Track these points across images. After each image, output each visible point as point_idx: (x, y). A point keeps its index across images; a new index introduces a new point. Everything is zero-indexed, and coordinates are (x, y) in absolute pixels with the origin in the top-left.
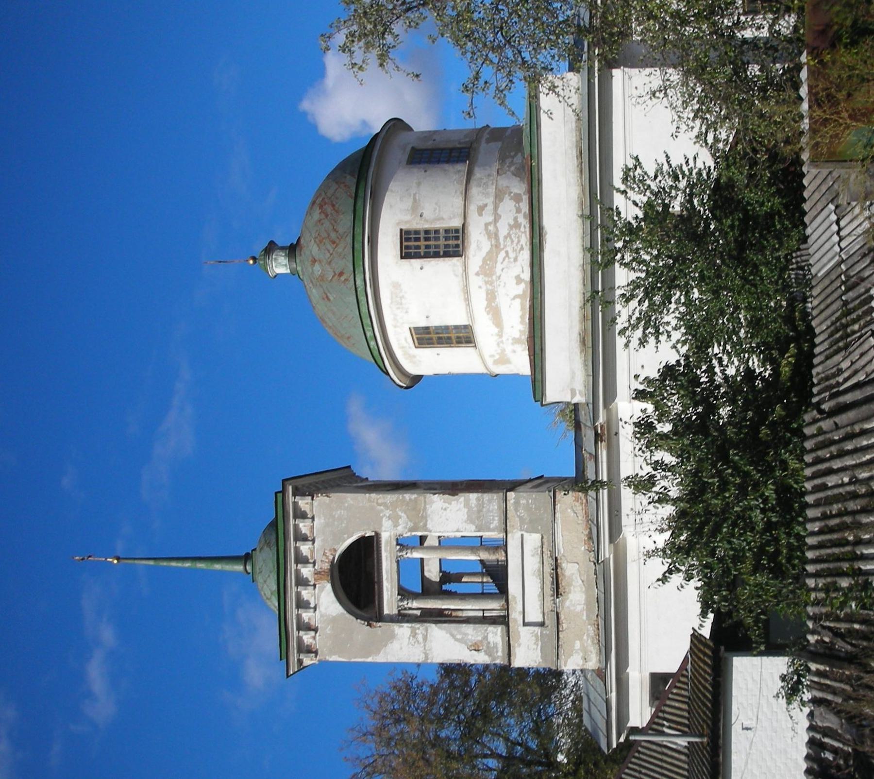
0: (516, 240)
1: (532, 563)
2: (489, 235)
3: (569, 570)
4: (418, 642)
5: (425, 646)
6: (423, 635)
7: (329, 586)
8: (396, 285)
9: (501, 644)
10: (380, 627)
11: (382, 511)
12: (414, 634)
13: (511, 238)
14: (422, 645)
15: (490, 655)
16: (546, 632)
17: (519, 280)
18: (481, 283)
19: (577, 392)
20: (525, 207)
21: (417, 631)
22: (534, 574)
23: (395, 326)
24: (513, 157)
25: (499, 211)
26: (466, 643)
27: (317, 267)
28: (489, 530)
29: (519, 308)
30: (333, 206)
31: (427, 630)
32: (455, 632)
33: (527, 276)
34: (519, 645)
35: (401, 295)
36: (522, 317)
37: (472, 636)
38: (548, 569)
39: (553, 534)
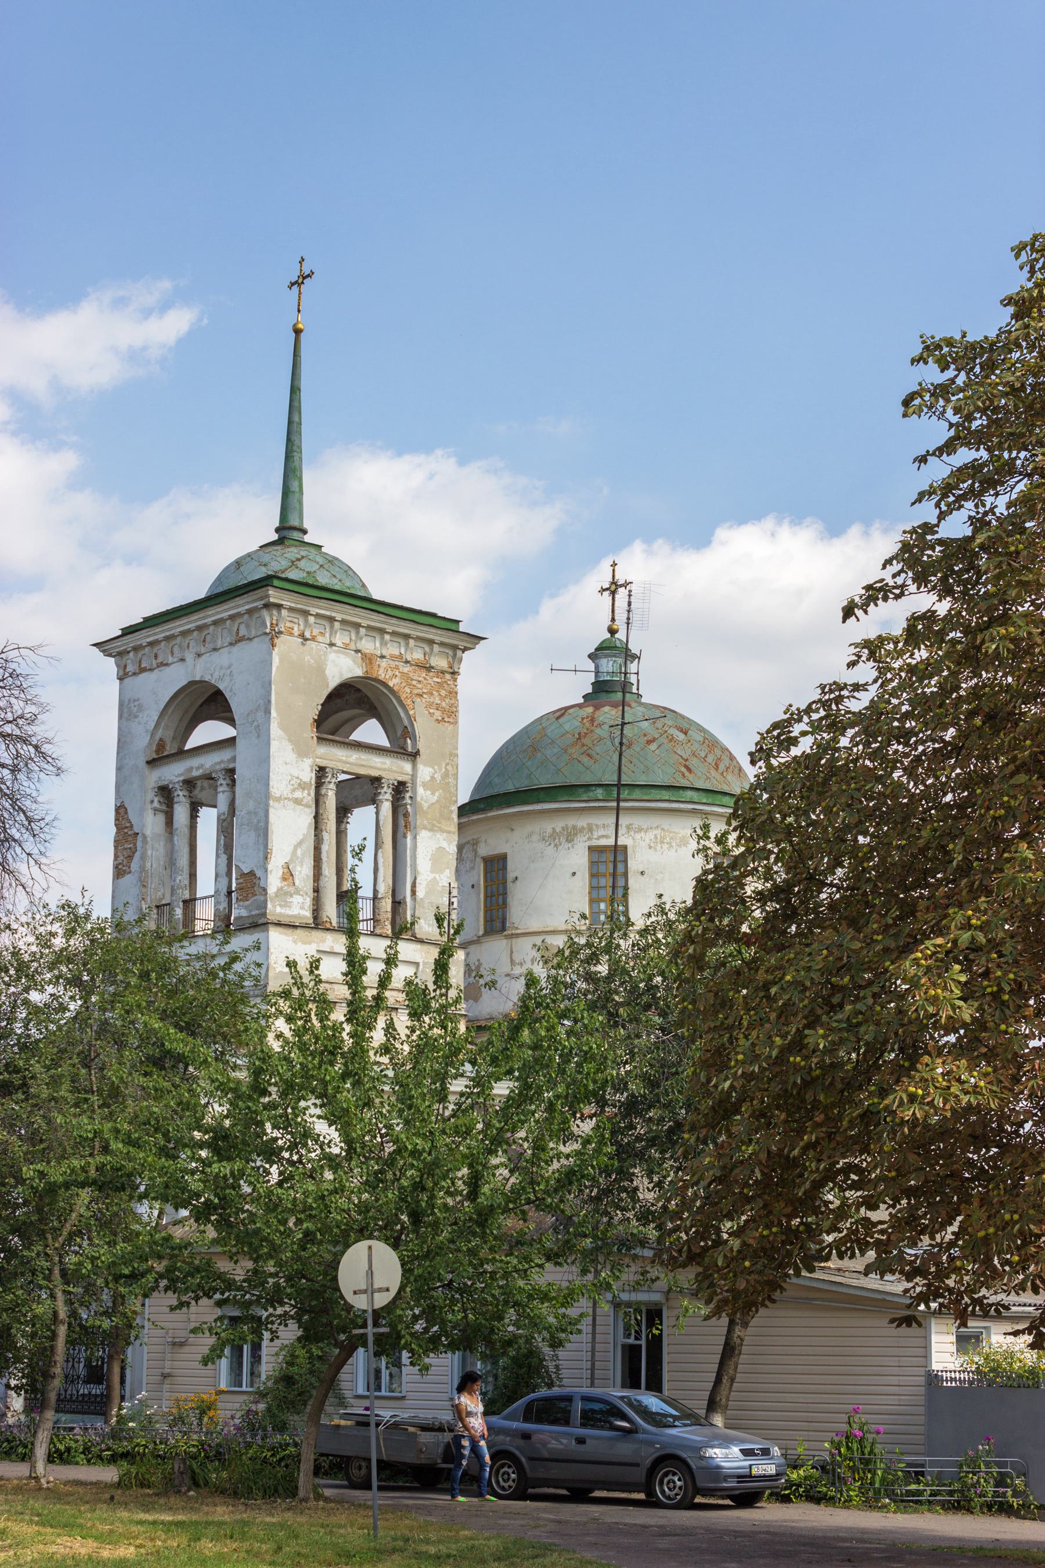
4: (293, 790)
5: (289, 799)
6: (302, 800)
9: (290, 913)
11: (440, 770)
12: (302, 786)
14: (290, 796)
15: (277, 895)
26: (291, 860)
31: (307, 806)
32: (304, 846)
34: (295, 942)
35: (674, 844)
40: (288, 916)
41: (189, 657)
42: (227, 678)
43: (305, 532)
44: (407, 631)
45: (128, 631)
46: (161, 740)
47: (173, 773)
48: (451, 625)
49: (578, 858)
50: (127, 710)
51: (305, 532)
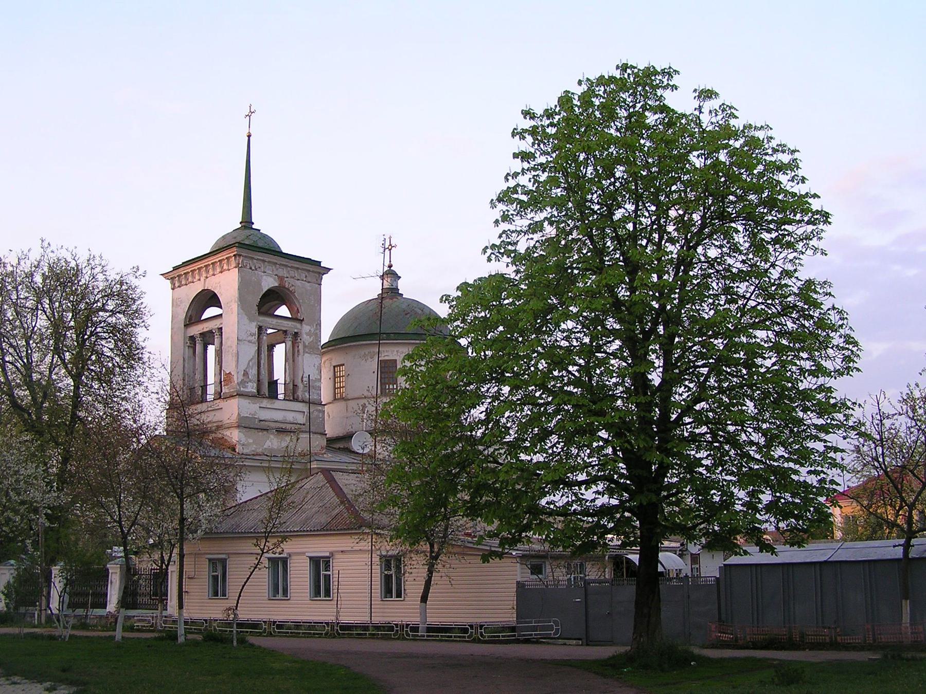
1: (290, 417)
7: (276, 284)
9: (247, 390)
12: (252, 335)
26: (246, 368)
32: (253, 361)
34: (249, 403)
38: (288, 427)
41: (202, 279)
42: (218, 287)
43: (253, 223)
44: (298, 266)
45: (175, 268)
46: (190, 316)
47: (196, 330)
48: (318, 263)
49: (374, 365)
50: (175, 303)
51: (253, 223)
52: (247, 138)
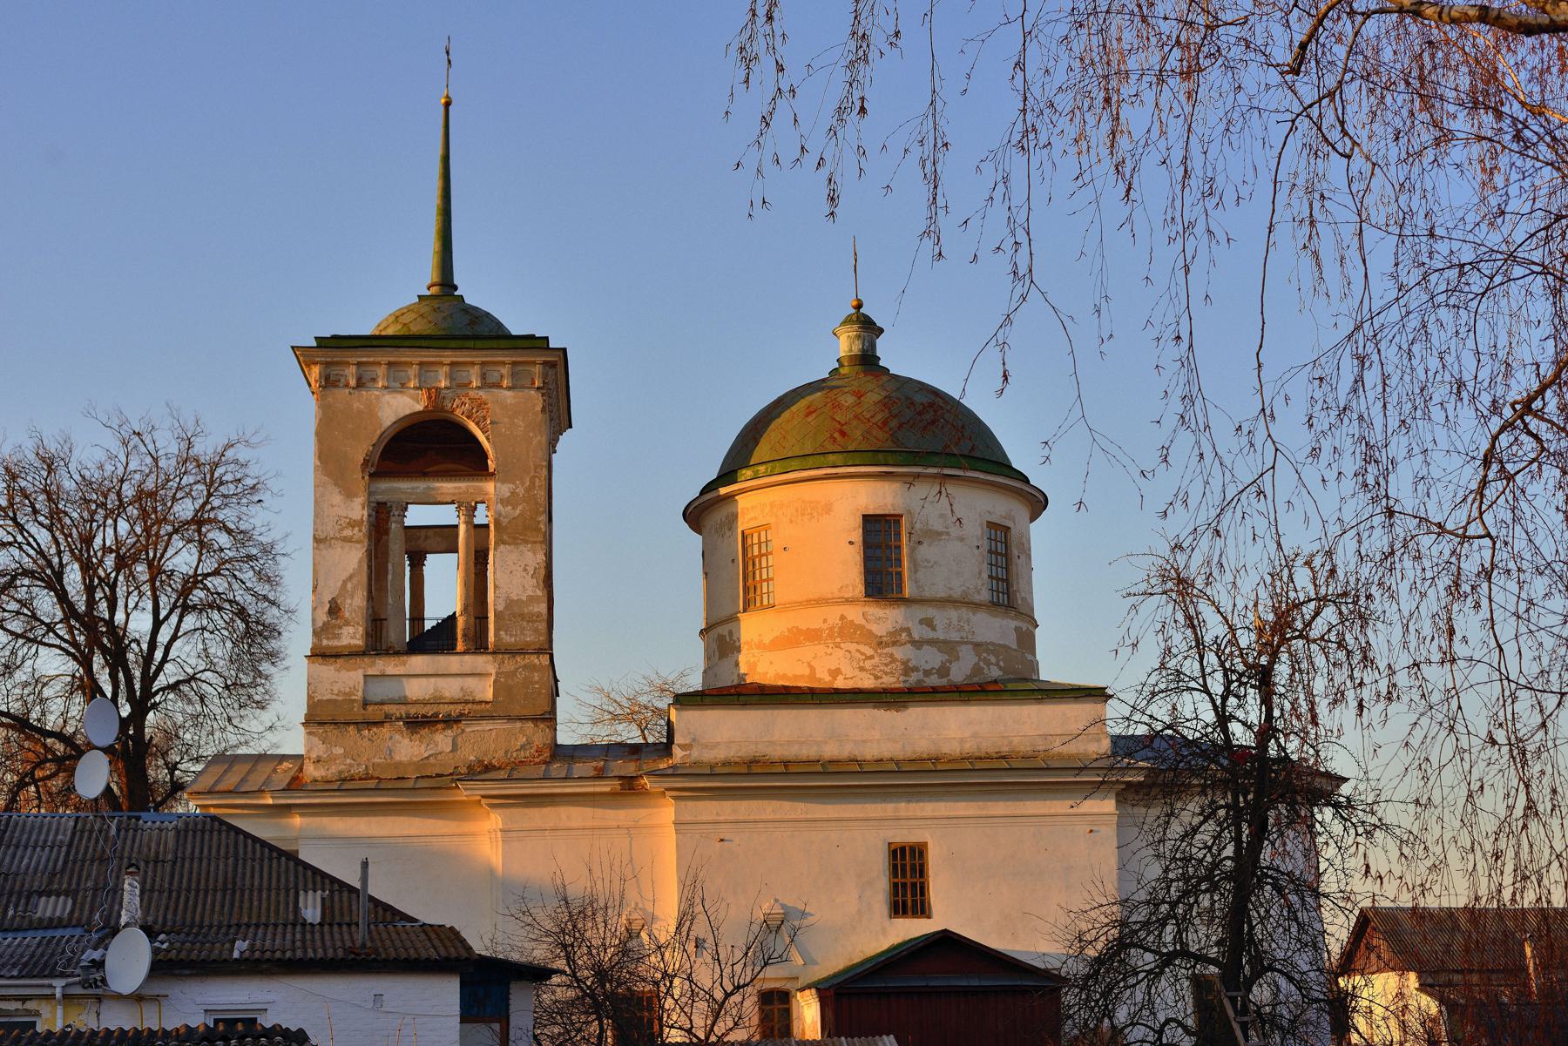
0: (887, 669)
1: (451, 689)
2: (895, 633)
3: (442, 740)
4: (342, 529)
6: (352, 537)
7: (419, 407)
8: (828, 509)
10: (363, 478)
12: (352, 524)
13: (891, 662)
14: (338, 535)
16: (357, 708)
17: (835, 673)
18: (830, 621)
19: (688, 752)
20: (933, 681)
21: (357, 529)
22: (436, 690)
23: (772, 505)
24: (997, 664)
25: (926, 647)
27: (850, 400)
28: (497, 630)
29: (799, 673)
30: (933, 422)
32: (355, 580)
33: (840, 683)
35: (815, 514)
36: (784, 676)
37: (351, 605)
38: (444, 710)
39: (492, 718)
40: (337, 647)
52: (442, 109)
